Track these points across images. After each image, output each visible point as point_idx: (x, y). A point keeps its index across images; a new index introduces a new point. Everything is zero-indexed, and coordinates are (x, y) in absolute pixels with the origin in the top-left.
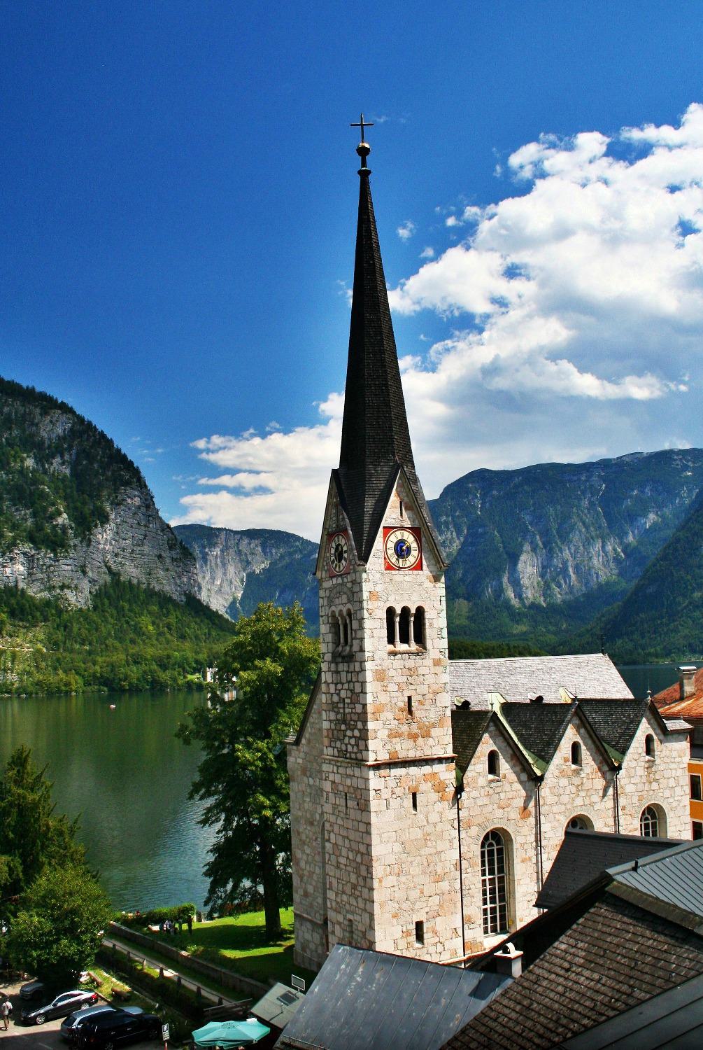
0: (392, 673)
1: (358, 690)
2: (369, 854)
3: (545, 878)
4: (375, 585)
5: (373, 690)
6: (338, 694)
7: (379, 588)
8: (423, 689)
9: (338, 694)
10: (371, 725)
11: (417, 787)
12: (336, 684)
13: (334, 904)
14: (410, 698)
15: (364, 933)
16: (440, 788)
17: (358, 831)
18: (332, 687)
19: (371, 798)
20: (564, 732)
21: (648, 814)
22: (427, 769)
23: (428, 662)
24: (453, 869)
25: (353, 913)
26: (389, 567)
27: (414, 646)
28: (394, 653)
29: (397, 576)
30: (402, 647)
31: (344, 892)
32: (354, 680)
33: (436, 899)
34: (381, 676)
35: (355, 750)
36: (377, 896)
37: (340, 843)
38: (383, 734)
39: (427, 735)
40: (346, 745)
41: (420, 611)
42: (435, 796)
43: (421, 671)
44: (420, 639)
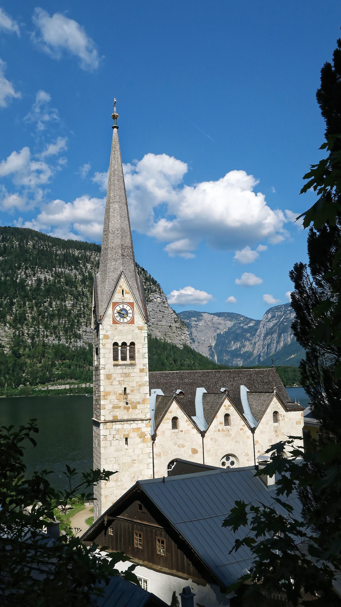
0: (114, 376)
4: (107, 331)
7: (109, 333)
8: (134, 384)
10: (102, 402)
16: (142, 436)
19: (101, 440)
22: (134, 425)
23: (137, 369)
26: (115, 322)
27: (128, 362)
28: (115, 365)
29: (119, 327)
30: (120, 362)
34: (109, 377)
39: (135, 408)
41: (133, 344)
42: (139, 440)
43: (132, 375)
44: (132, 357)
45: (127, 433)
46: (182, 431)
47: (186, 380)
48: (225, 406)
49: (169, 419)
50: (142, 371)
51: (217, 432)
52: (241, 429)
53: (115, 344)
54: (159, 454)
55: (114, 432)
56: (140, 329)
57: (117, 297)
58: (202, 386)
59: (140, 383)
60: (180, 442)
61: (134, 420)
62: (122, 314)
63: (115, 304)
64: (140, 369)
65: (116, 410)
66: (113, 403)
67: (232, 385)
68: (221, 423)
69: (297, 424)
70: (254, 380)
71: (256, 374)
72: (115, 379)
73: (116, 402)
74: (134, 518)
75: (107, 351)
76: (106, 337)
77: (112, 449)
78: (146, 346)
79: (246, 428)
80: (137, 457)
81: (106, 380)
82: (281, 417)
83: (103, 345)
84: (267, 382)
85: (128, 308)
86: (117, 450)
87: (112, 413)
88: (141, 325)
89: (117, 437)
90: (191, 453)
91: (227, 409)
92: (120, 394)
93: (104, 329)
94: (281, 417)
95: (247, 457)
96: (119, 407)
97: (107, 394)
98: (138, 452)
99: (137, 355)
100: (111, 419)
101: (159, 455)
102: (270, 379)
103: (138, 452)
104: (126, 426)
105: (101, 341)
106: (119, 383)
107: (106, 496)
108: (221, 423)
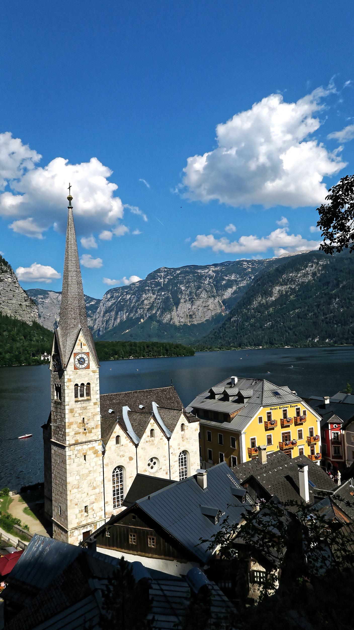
0: (75, 410)
1: (63, 416)
2: (66, 481)
3: (125, 495)
4: (70, 376)
5: (68, 418)
6: (57, 416)
7: (71, 377)
8: (90, 414)
9: (57, 416)
10: (67, 431)
11: (86, 453)
12: (56, 412)
13: (55, 499)
14: (83, 418)
15: (64, 512)
16: (96, 452)
17: (62, 471)
18: (55, 413)
19: (67, 459)
20: (147, 426)
21: (183, 454)
22: (90, 445)
23: (92, 403)
24: (100, 484)
25: (61, 503)
26: (76, 368)
27: (85, 398)
28: (76, 401)
29: (79, 372)
30: (80, 398)
31: (58, 495)
32: (62, 412)
33: (93, 497)
34: (72, 411)
35: (62, 439)
36: (69, 498)
37: (57, 475)
38: (72, 433)
39: (90, 432)
40: (59, 437)
41: (89, 384)
42: (93, 456)
43: (88, 408)
44: (88, 394)
45: (85, 452)
46: (122, 445)
47: (114, 401)
48: (151, 424)
49: (113, 438)
50: (95, 404)
51: (146, 443)
52: (161, 439)
53: (76, 385)
54: (107, 464)
55: (76, 452)
56: (94, 372)
57: (77, 349)
58: (126, 405)
59: (94, 414)
60: (121, 453)
61: (90, 442)
62: (82, 361)
63: (76, 354)
64: (94, 403)
65: (77, 435)
66: (75, 430)
67: (147, 402)
68: (148, 436)
69: (195, 431)
70: (160, 397)
71: (161, 392)
72: (76, 412)
73: (77, 429)
74: (129, 525)
75: (70, 391)
76: (70, 380)
77: (75, 464)
78: (98, 385)
79: (164, 438)
80: (92, 469)
81: (70, 414)
82: (186, 427)
83: (67, 386)
84: (169, 398)
85: (85, 356)
86: (79, 465)
87: (74, 438)
88: (94, 370)
89: (78, 455)
90: (128, 460)
91: (152, 426)
92: (80, 423)
93: (68, 375)
94: (186, 427)
95: (164, 458)
96: (80, 433)
97: (71, 424)
98: (92, 464)
99: (92, 392)
100: (74, 442)
101: (107, 465)
102: (171, 395)
103: (92, 464)
104: (85, 447)
105: (65, 384)
106: (79, 415)
107: (71, 500)
108: (148, 436)
